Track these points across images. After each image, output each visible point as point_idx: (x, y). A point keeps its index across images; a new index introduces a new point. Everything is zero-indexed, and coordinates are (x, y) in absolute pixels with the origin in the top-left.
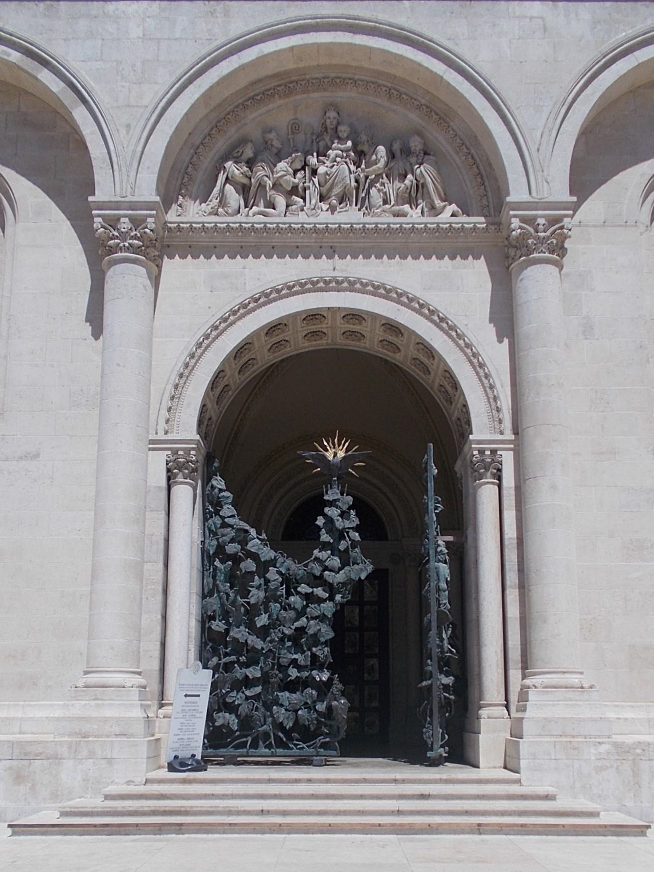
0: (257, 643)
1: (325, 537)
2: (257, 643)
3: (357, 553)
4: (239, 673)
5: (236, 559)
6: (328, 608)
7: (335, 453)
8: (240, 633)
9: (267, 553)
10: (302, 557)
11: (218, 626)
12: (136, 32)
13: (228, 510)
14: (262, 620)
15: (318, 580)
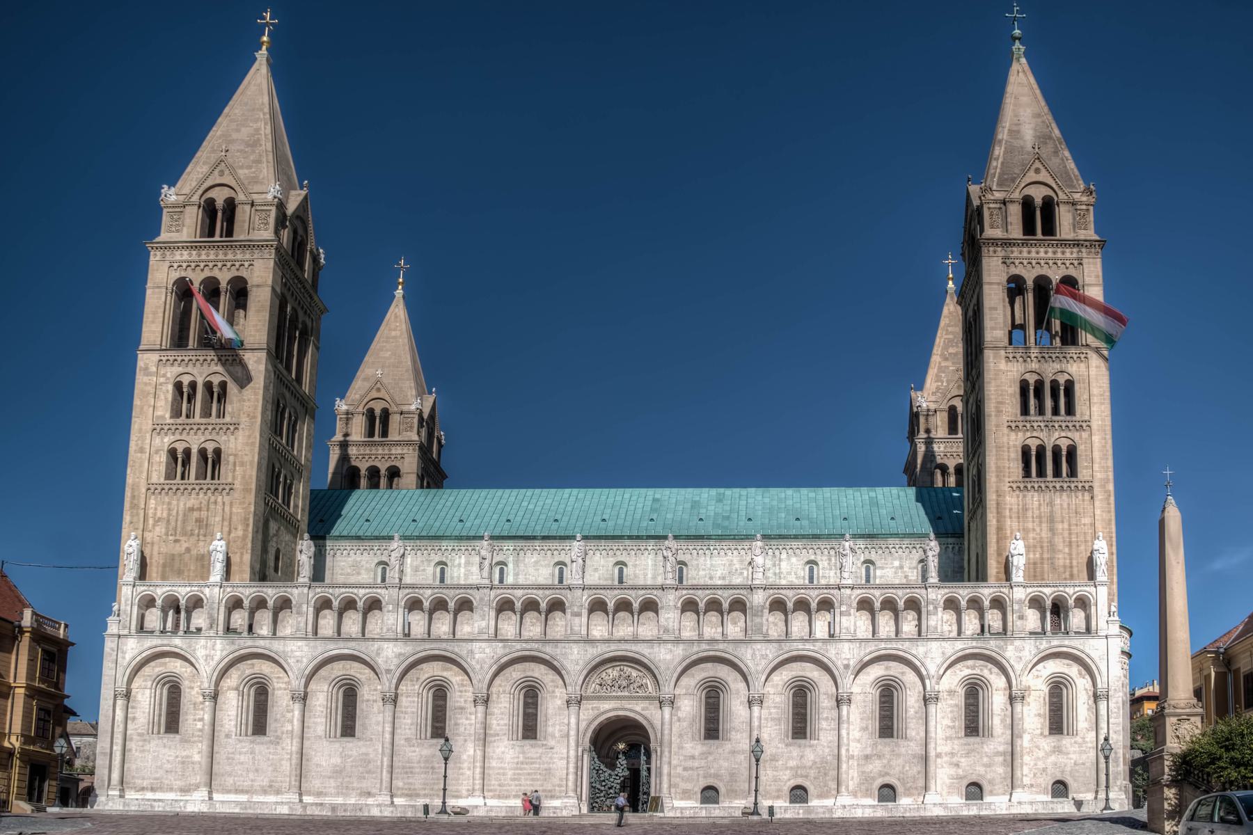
0: (603, 788)
1: (619, 765)
2: (603, 788)
3: (626, 769)
4: (598, 795)
5: (598, 770)
6: (619, 781)
7: (621, 746)
8: (598, 786)
9: (605, 769)
10: (614, 770)
11: (594, 785)
12: (576, 652)
13: (596, 759)
14: (604, 784)
15: (617, 775)
